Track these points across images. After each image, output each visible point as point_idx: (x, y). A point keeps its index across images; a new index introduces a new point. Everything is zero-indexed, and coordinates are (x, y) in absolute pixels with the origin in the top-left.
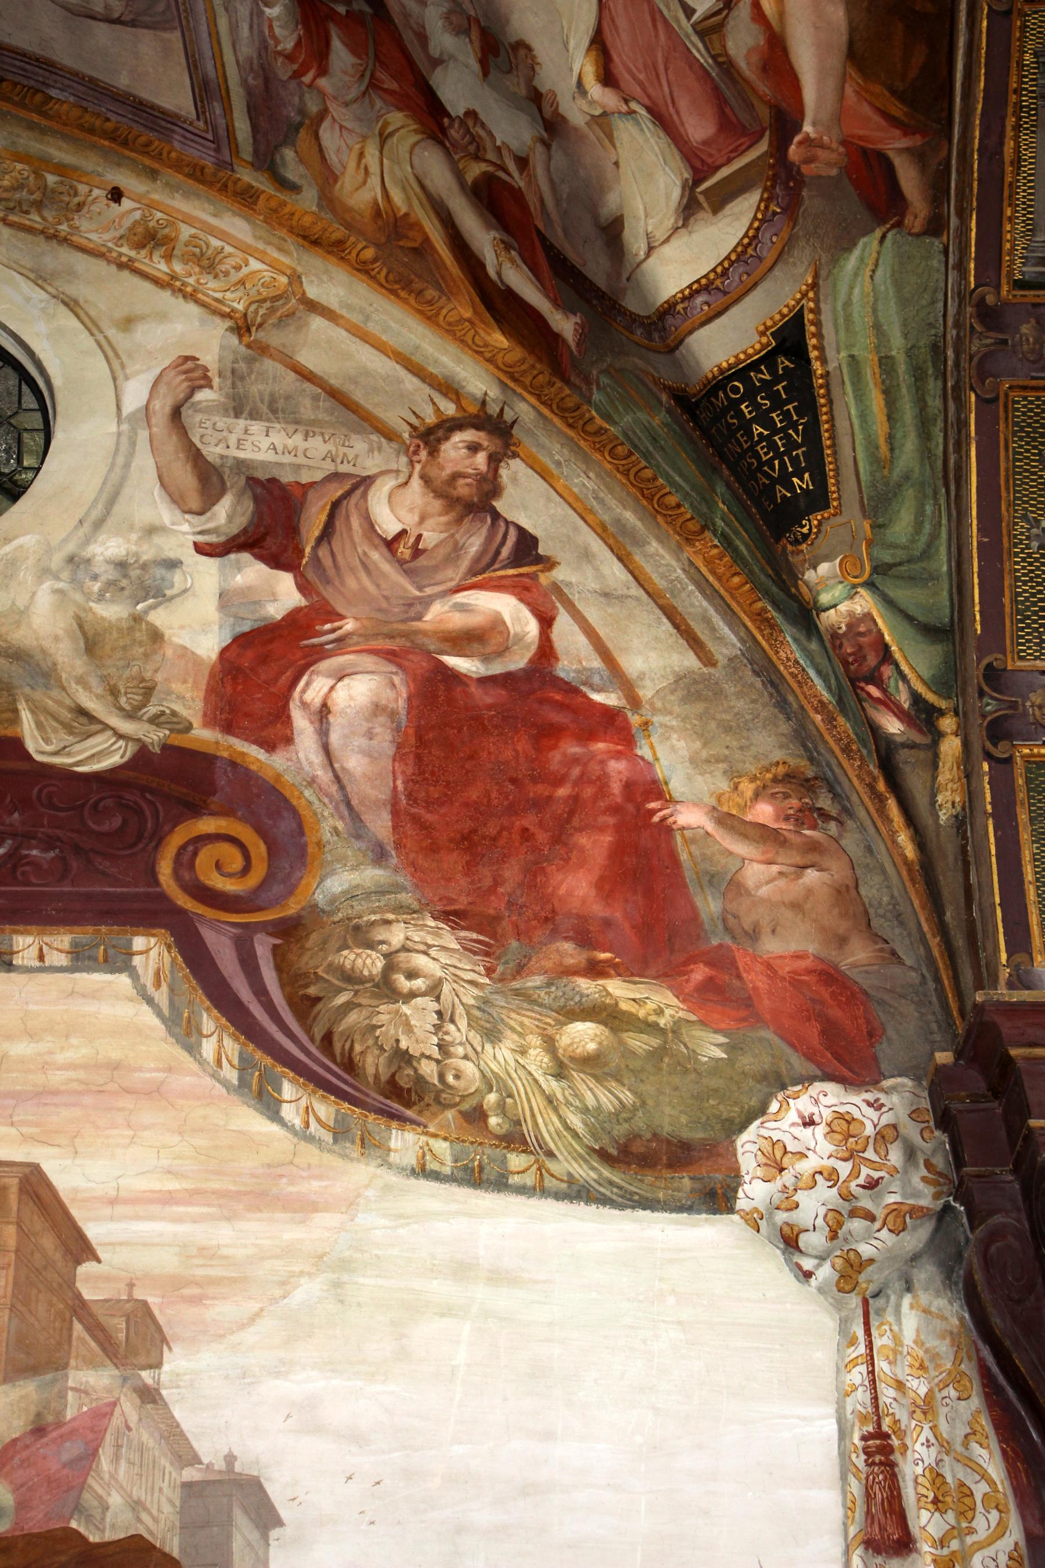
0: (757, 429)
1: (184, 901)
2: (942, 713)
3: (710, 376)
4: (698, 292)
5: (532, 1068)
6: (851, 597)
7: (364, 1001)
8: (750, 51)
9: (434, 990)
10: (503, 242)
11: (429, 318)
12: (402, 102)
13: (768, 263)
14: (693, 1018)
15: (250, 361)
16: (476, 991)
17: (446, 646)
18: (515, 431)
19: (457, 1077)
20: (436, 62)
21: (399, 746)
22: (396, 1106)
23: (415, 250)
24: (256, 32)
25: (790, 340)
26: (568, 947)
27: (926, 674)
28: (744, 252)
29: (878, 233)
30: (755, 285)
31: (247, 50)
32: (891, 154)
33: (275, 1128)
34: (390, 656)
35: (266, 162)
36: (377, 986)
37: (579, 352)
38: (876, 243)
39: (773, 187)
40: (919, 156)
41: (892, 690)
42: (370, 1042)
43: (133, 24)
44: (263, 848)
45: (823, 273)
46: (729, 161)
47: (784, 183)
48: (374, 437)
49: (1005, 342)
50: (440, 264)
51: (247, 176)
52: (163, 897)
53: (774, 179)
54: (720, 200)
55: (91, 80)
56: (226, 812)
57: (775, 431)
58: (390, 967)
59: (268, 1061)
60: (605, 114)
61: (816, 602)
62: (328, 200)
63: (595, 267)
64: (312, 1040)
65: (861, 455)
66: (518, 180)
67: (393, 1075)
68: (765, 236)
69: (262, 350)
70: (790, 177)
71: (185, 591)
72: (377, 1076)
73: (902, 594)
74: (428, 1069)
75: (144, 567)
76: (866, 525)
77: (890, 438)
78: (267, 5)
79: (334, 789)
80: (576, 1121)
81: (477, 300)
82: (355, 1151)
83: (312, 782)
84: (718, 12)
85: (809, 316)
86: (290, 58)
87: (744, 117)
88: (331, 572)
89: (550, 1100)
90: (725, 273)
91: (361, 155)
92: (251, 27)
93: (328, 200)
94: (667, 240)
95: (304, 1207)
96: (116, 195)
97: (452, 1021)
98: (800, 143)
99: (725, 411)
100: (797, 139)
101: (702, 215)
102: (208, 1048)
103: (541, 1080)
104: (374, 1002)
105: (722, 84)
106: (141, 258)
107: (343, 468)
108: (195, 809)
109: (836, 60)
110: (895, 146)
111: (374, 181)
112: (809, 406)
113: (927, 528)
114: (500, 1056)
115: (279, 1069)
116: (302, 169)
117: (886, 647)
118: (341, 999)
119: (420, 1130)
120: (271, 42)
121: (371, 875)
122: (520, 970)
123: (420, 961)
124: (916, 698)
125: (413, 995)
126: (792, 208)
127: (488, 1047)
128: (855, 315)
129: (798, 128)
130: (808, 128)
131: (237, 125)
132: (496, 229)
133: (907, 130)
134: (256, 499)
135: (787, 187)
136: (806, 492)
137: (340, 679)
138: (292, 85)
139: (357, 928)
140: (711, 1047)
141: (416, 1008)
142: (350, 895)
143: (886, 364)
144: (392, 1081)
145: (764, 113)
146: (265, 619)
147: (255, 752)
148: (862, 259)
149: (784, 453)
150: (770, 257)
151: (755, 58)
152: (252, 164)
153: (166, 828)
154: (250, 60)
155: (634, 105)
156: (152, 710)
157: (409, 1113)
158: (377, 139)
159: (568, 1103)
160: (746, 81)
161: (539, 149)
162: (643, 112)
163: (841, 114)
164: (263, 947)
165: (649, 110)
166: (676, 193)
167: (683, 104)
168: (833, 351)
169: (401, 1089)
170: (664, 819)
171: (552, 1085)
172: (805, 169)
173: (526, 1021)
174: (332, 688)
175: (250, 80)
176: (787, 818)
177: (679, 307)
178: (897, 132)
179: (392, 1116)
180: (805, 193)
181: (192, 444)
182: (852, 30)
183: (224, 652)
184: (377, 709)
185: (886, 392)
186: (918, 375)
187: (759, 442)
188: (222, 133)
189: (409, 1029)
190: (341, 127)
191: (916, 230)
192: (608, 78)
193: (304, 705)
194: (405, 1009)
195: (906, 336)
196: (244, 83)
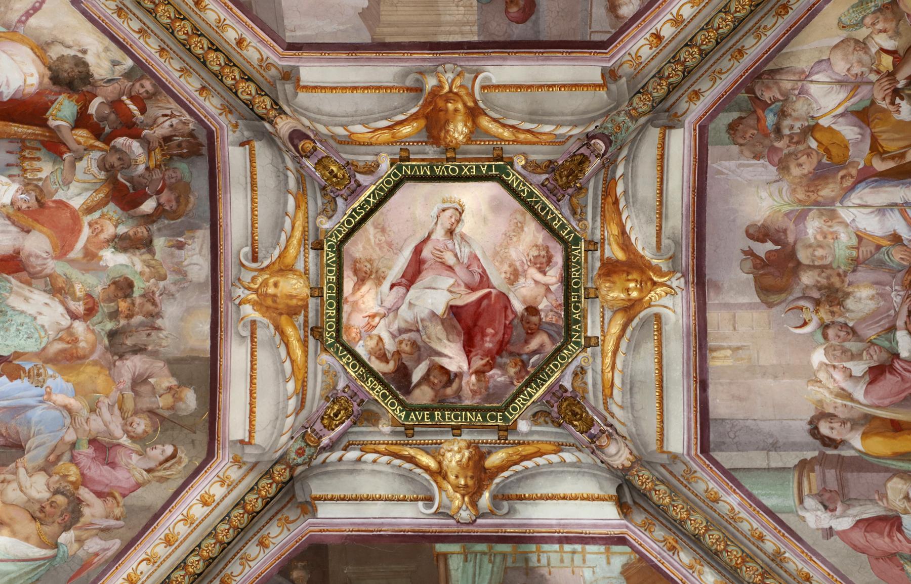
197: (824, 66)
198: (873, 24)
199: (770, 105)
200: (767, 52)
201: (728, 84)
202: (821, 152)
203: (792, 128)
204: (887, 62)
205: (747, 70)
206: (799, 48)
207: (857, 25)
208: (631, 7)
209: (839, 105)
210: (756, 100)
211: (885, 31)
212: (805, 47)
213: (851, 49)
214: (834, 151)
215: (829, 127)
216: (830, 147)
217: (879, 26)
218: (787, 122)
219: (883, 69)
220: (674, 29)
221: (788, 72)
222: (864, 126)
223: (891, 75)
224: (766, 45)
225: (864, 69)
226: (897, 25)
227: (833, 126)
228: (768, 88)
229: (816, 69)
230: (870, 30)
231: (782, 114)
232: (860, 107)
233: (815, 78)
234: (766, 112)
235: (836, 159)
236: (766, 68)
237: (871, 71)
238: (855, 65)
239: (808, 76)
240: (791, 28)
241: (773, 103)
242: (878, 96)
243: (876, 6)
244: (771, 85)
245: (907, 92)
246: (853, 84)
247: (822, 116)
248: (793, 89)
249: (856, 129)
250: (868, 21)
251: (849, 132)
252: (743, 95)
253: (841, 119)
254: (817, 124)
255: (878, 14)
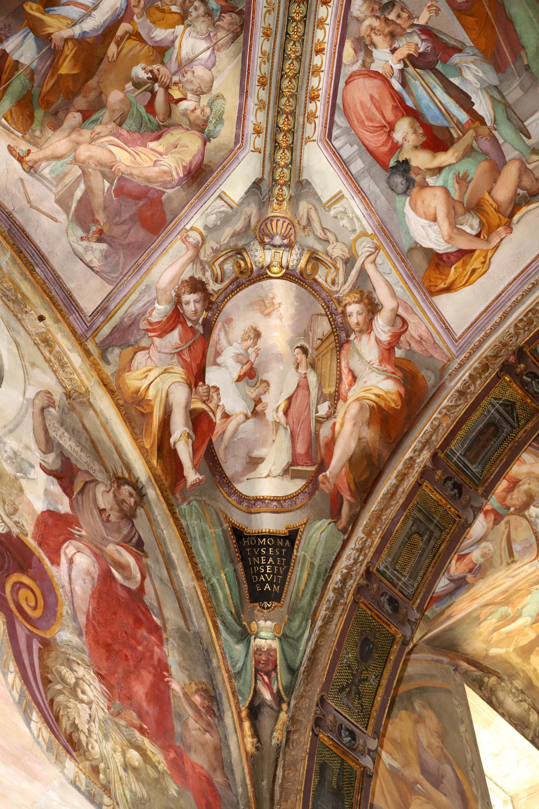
0: (271, 560)
1: (12, 606)
2: (284, 702)
3: (264, 531)
4: (275, 500)
5: (117, 760)
6: (273, 640)
7: (66, 693)
8: (325, 437)
9: (90, 703)
10: (188, 434)
11: (134, 439)
12: (186, 366)
13: (298, 507)
14: (169, 772)
15: (69, 410)
16: (103, 714)
17: (112, 563)
18: (144, 498)
19: (92, 748)
20: (215, 364)
21: (93, 593)
22: (70, 747)
23: (143, 414)
24: (145, 308)
25: (292, 536)
26: (134, 715)
27: (284, 684)
28: (293, 498)
29: (329, 521)
30: (291, 511)
31: (136, 310)
32: (344, 499)
33: (27, 730)
34: (95, 555)
35: (104, 348)
36: (71, 689)
37: (190, 488)
38: (327, 524)
39: (310, 483)
40: (351, 506)
41: (272, 682)
42: (66, 713)
43: (97, 273)
44: (42, 603)
45: (309, 522)
46: (302, 465)
47: (313, 483)
48: (102, 467)
49: (368, 586)
50: (150, 424)
51: (90, 346)
52: (5, 599)
53: (311, 481)
54: (296, 475)
55: (58, 277)
56: (34, 579)
57: (276, 565)
58: (76, 684)
59: (30, 698)
60: (279, 423)
61: (257, 633)
62: (118, 374)
63: (231, 466)
64: (47, 698)
65: (294, 591)
66: (218, 419)
67: (71, 733)
68: (301, 497)
69: (73, 409)
70: (315, 484)
71: (34, 479)
72: (65, 729)
73: (286, 648)
74: (83, 738)
75: (22, 459)
76: (287, 617)
77: (303, 591)
78: (158, 303)
79: (70, 595)
80: (128, 793)
81: (156, 445)
82: (53, 759)
83: (63, 587)
84: (324, 418)
85: (300, 533)
86: (150, 324)
87: (313, 455)
88: (81, 508)
89: (121, 779)
90: (285, 500)
91: (150, 370)
92: (145, 305)
93: (118, 374)
94: (275, 477)
95: (32, 776)
96: (41, 318)
97: (94, 722)
98: (324, 476)
99: (262, 546)
100: (323, 474)
101: (288, 476)
102: (11, 677)
103: (119, 768)
104: (70, 696)
105: (313, 439)
106: (42, 345)
107: (90, 471)
108: (23, 570)
109: (345, 458)
110: (347, 497)
111: (146, 382)
112: (288, 563)
113: (301, 630)
114: (108, 747)
115: (33, 704)
116: (117, 359)
117: (276, 666)
118: (59, 687)
119: (76, 764)
120: (148, 315)
121: (75, 640)
122: (118, 714)
123: (87, 688)
124: (278, 691)
125: (82, 701)
126: (311, 494)
127: (104, 741)
128: (311, 542)
129: (325, 471)
130: (328, 473)
131: (104, 328)
132: (189, 428)
133: (352, 495)
134: (62, 461)
135: (313, 487)
136: (276, 592)
137: (79, 552)
138: (143, 332)
139: (68, 659)
140: (173, 789)
141: (82, 707)
142: (68, 644)
143: (312, 564)
144: (70, 735)
145: (319, 459)
146: (58, 510)
147: (47, 562)
148: (321, 526)
149: (275, 574)
150: (299, 505)
151: (325, 440)
152: (97, 344)
153: (12, 571)
154: (133, 314)
155: (288, 427)
156: (15, 518)
157: (74, 754)
158: (162, 370)
159: (126, 784)
160: (320, 445)
161: (242, 417)
162: (289, 431)
163: (338, 476)
164: (36, 645)
165: (291, 432)
166: (285, 464)
167: (300, 437)
168: (302, 551)
169: (73, 741)
170: (168, 682)
171: (122, 772)
172: (321, 484)
173: (118, 738)
174: (75, 553)
175: (126, 320)
176: (204, 707)
177: (267, 501)
178: (349, 494)
179: (68, 752)
180: (317, 492)
181: (45, 426)
182: (354, 453)
183: (43, 512)
184: (88, 573)
185: (309, 574)
186: (319, 577)
187: (269, 565)
188: (95, 327)
189: (79, 716)
190: (150, 357)
191: (339, 528)
192: (286, 413)
193: (65, 554)
194: (79, 705)
195: (321, 560)
196: (122, 319)
197: (210, 64)
198: (203, 110)
199: (221, 14)
200: (251, 47)
201: (257, 7)
202: (166, 8)
203: (196, 9)
204: (176, 94)
205: (253, 25)
206: (233, 64)
207: (212, 103)
208: (357, 7)
209: (180, 46)
210: (232, 9)
211: (193, 111)
212: (230, 67)
213: (203, 86)
214: (159, 15)
215: (174, 27)
216: (164, 14)
217: (198, 112)
218: (202, 10)
219: (176, 88)
220: (320, 17)
221: (227, 43)
222: (156, 45)
223: (167, 88)
224: (255, 51)
225: (185, 80)
226: (189, 120)
227: (172, 30)
228: (231, 24)
229: (212, 58)
230: (202, 105)
231: (209, 13)
232: (167, 54)
233: (209, 52)
234: (219, 7)
235: (153, 10)
236: (242, 36)
237: (180, 82)
238: (192, 78)
239: (213, 50)
240: (249, 73)
241: (220, 16)
242: (163, 70)
243: (211, 122)
244: (230, 27)
245: (149, 85)
246: (184, 65)
247: (184, 31)
248: (215, 35)
249: (158, 39)
250: (208, 110)
251: (161, 34)
252: (242, 6)
253: (172, 38)
254: (183, 24)
255: (205, 118)
